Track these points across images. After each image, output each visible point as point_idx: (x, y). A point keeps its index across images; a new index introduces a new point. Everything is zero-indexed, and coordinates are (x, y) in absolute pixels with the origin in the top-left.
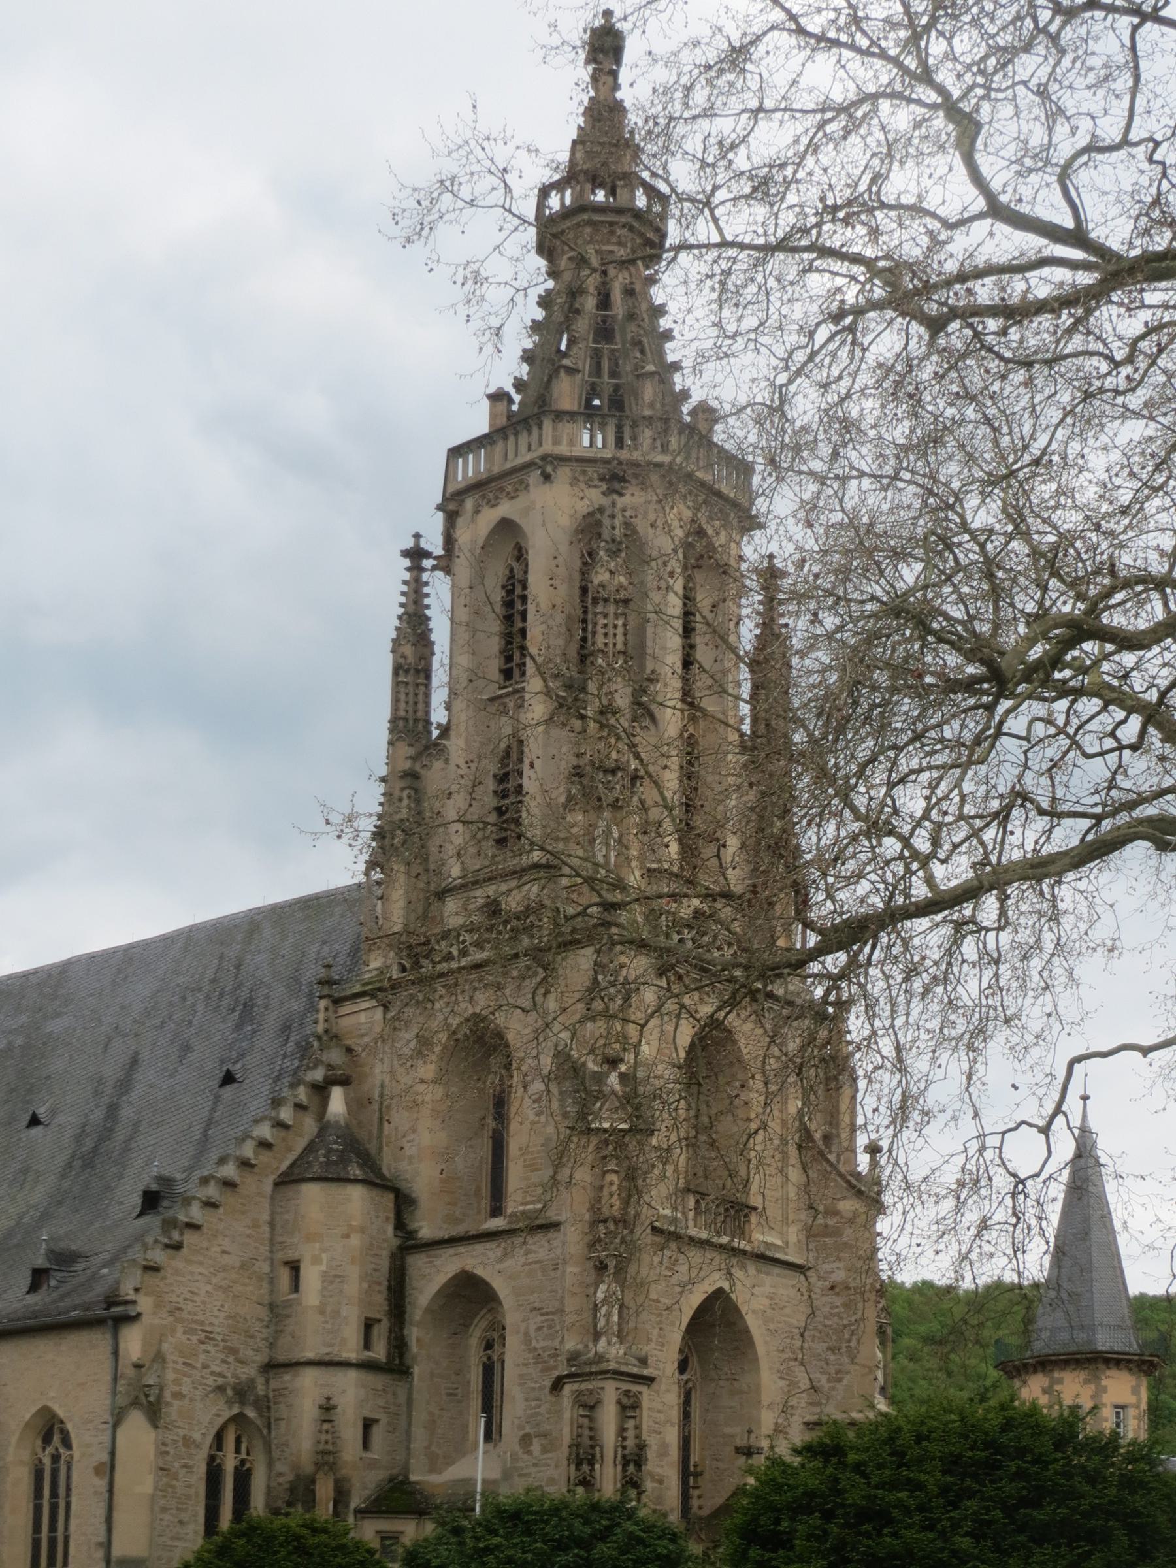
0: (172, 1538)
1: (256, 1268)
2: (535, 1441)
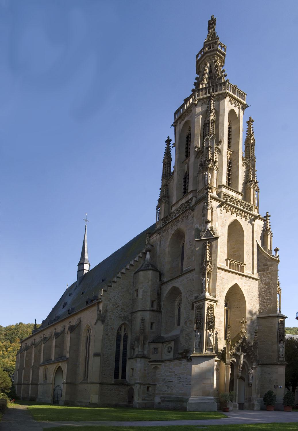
0: (108, 349)
2: (188, 322)
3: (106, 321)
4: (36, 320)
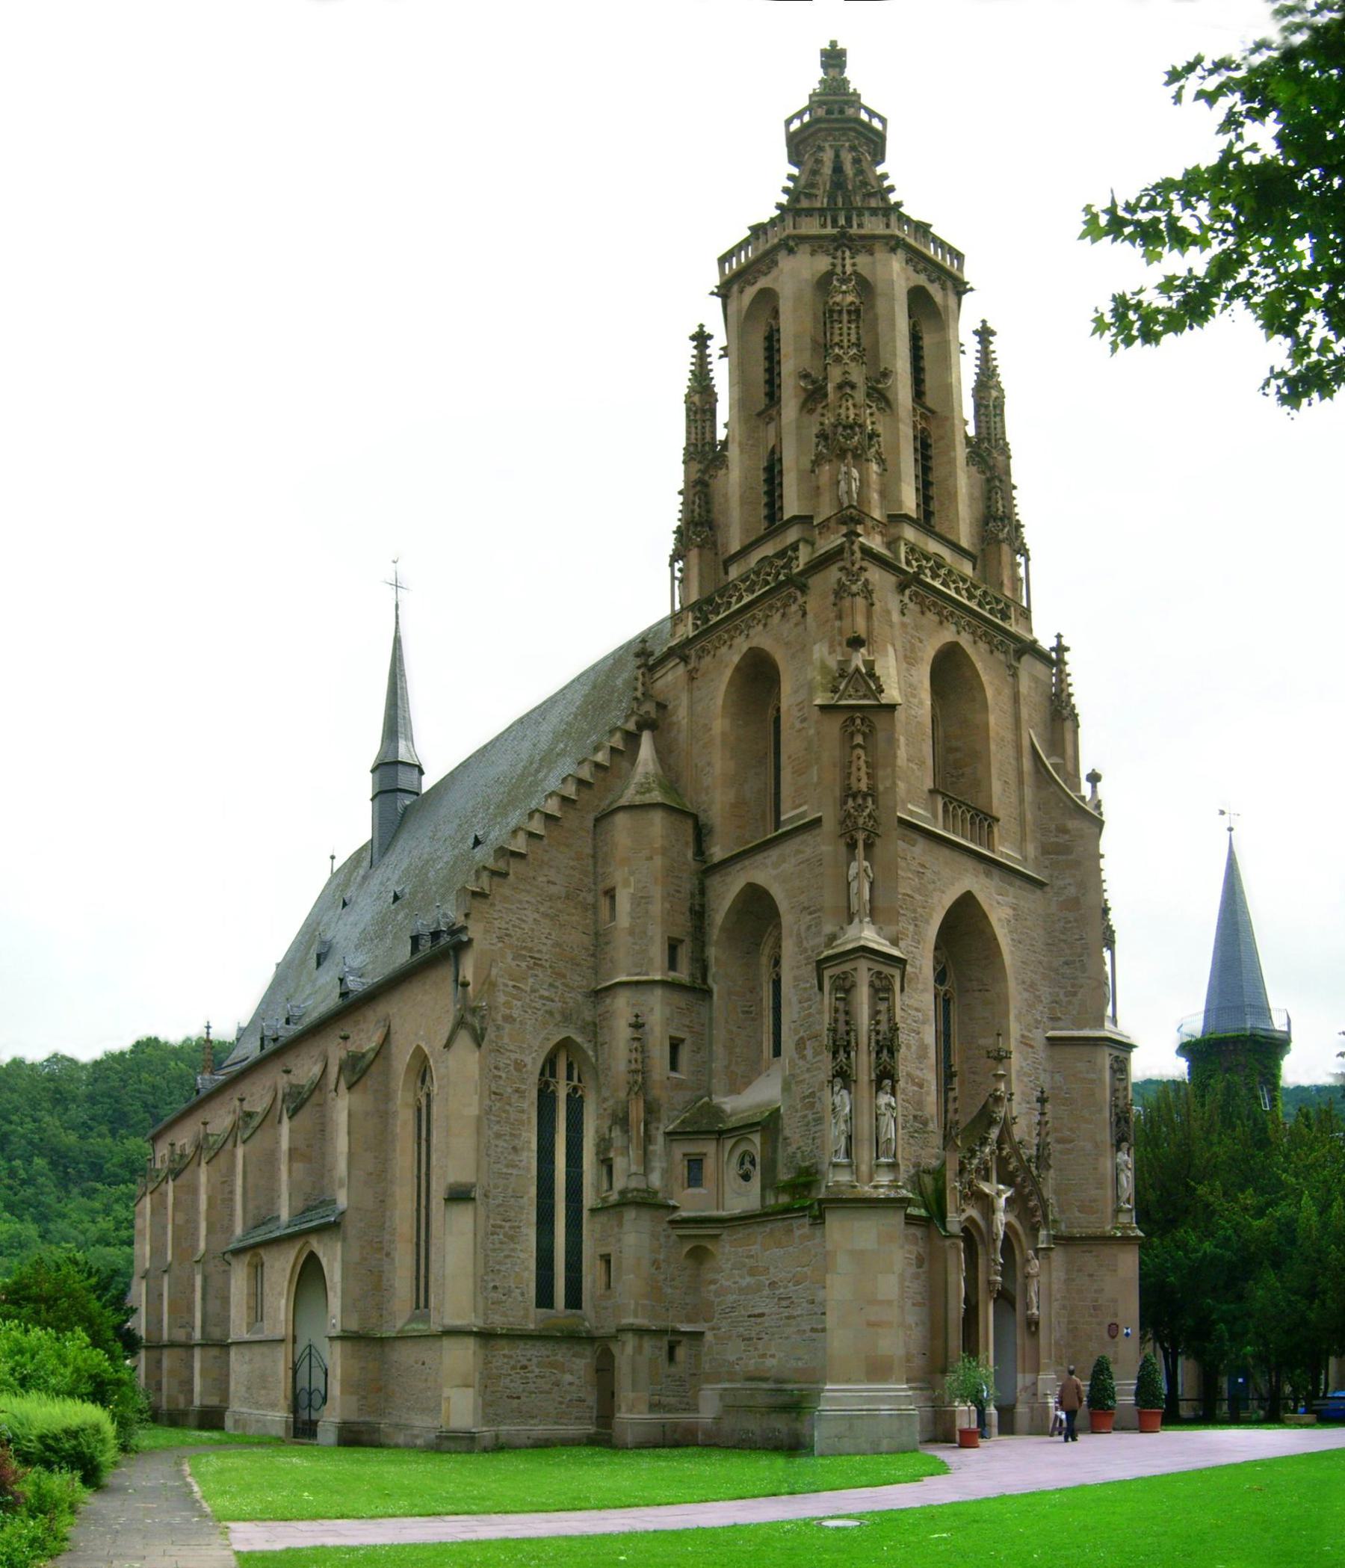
0: (507, 1166)
1: (580, 898)
2: (808, 1043)
3: (491, 1034)
4: (208, 1027)
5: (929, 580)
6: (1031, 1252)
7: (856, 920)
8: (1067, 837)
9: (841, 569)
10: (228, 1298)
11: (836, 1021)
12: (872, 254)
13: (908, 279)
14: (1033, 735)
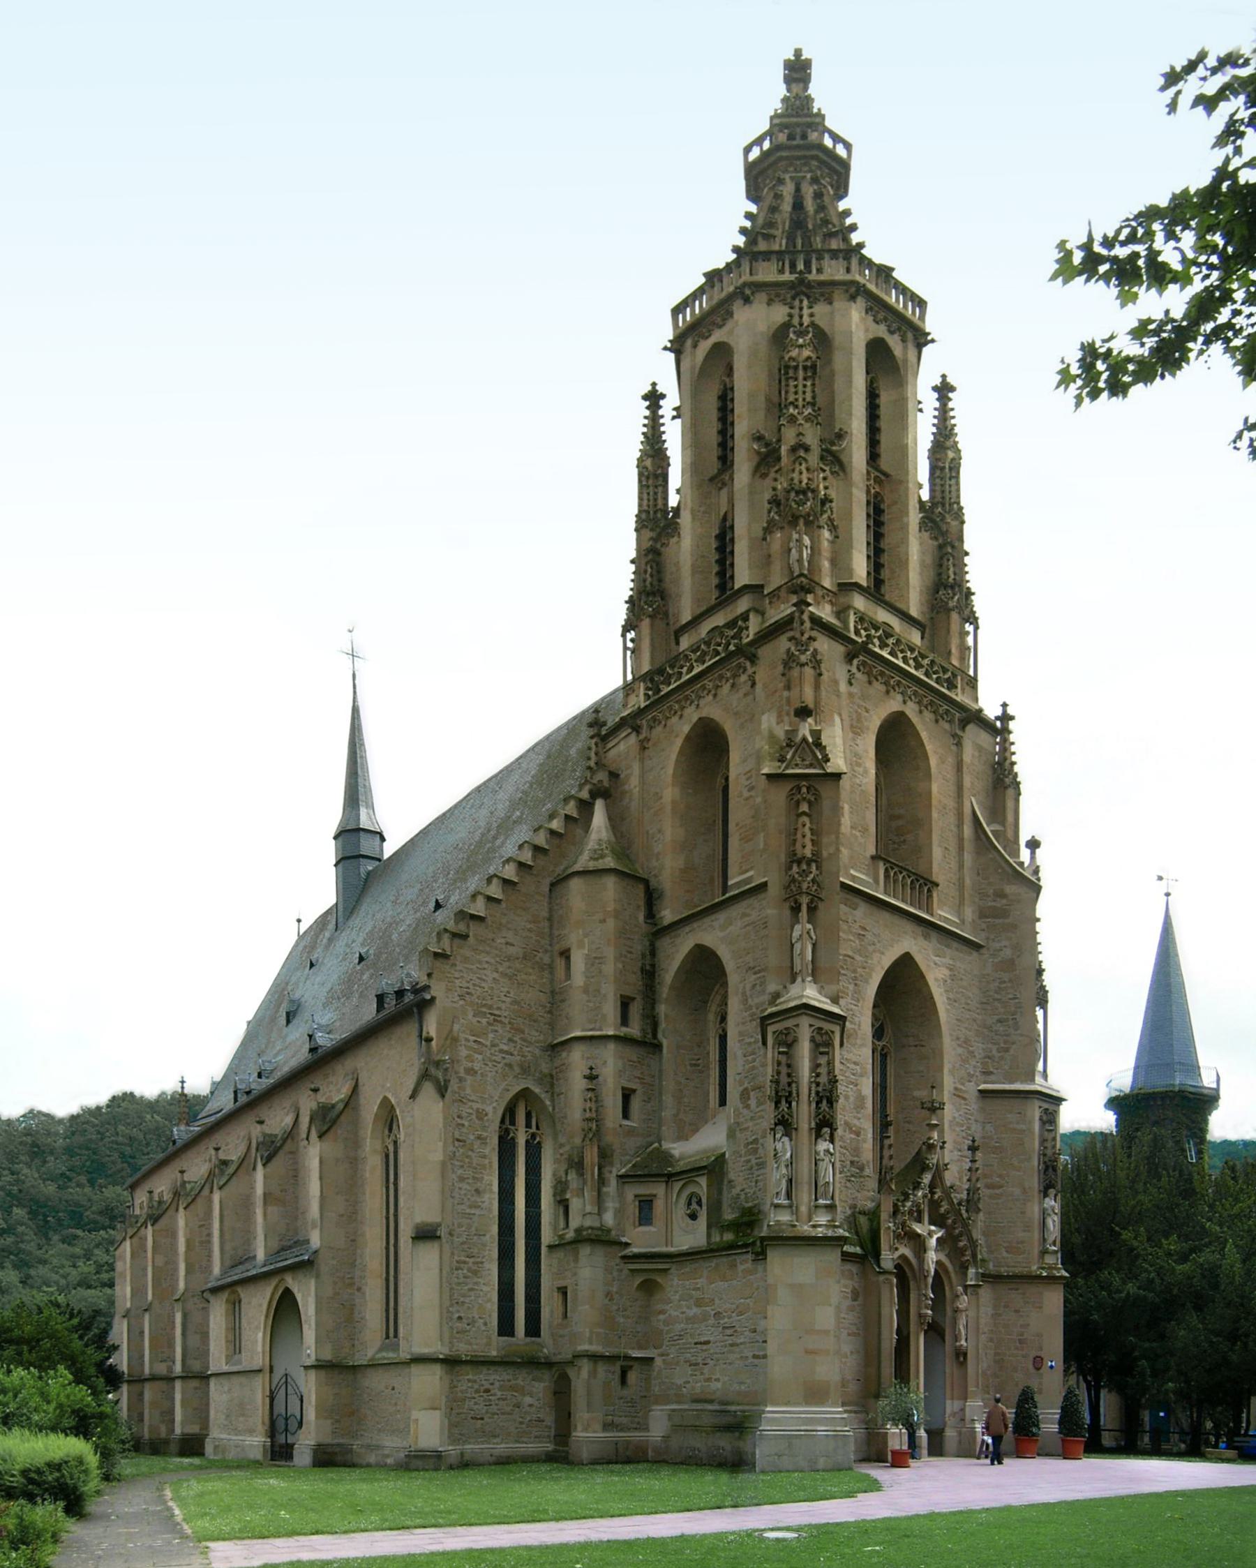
0: (470, 1207)
1: (537, 959)
2: (752, 1094)
3: (454, 1085)
5: (877, 650)
6: (960, 1289)
7: (799, 979)
8: (1004, 901)
9: (790, 639)
10: (208, 1333)
11: (779, 1073)
12: (831, 303)
13: (867, 330)
14: (974, 803)
